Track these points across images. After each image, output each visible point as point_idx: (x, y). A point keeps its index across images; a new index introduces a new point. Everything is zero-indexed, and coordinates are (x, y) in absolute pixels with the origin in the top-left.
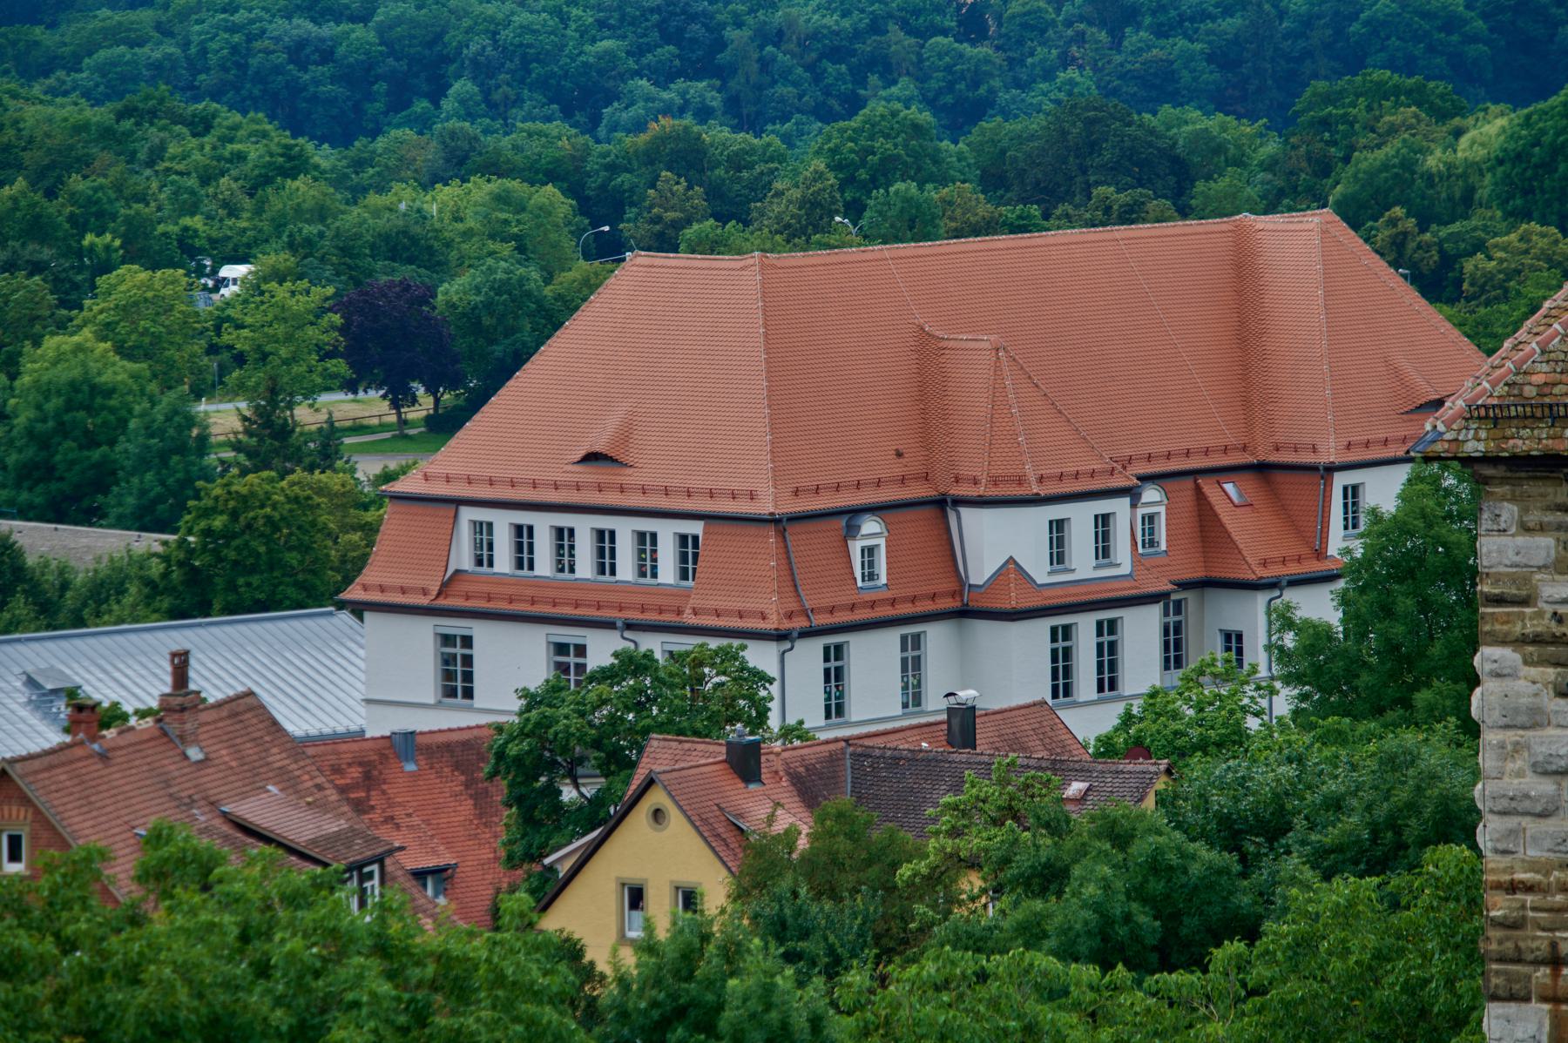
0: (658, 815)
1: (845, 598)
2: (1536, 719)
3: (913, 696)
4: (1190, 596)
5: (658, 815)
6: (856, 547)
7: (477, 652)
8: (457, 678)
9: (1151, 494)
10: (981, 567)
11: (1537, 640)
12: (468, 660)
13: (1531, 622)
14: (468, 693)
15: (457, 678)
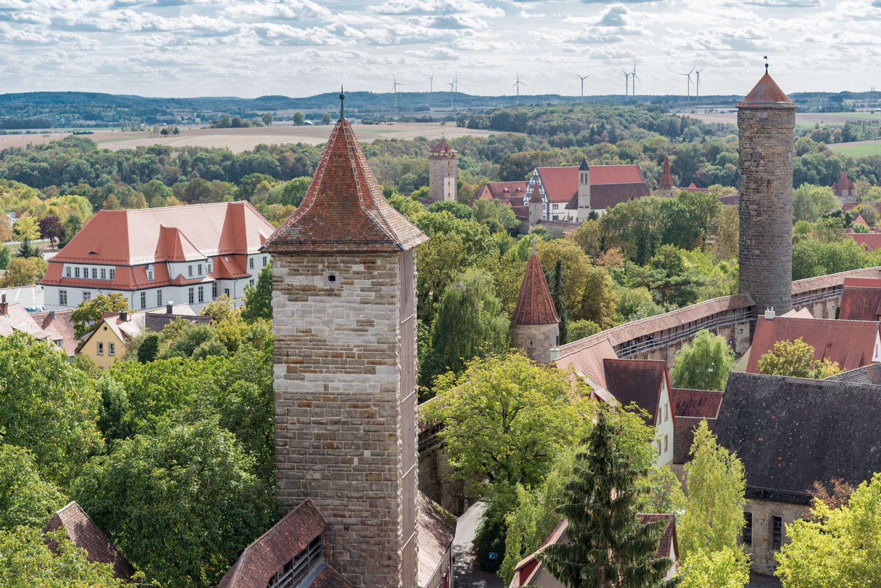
2: (284, 306)
5: (106, 329)
6: (147, 271)
8: (63, 301)
9: (210, 260)
10: (174, 277)
13: (283, 285)
15: (63, 301)
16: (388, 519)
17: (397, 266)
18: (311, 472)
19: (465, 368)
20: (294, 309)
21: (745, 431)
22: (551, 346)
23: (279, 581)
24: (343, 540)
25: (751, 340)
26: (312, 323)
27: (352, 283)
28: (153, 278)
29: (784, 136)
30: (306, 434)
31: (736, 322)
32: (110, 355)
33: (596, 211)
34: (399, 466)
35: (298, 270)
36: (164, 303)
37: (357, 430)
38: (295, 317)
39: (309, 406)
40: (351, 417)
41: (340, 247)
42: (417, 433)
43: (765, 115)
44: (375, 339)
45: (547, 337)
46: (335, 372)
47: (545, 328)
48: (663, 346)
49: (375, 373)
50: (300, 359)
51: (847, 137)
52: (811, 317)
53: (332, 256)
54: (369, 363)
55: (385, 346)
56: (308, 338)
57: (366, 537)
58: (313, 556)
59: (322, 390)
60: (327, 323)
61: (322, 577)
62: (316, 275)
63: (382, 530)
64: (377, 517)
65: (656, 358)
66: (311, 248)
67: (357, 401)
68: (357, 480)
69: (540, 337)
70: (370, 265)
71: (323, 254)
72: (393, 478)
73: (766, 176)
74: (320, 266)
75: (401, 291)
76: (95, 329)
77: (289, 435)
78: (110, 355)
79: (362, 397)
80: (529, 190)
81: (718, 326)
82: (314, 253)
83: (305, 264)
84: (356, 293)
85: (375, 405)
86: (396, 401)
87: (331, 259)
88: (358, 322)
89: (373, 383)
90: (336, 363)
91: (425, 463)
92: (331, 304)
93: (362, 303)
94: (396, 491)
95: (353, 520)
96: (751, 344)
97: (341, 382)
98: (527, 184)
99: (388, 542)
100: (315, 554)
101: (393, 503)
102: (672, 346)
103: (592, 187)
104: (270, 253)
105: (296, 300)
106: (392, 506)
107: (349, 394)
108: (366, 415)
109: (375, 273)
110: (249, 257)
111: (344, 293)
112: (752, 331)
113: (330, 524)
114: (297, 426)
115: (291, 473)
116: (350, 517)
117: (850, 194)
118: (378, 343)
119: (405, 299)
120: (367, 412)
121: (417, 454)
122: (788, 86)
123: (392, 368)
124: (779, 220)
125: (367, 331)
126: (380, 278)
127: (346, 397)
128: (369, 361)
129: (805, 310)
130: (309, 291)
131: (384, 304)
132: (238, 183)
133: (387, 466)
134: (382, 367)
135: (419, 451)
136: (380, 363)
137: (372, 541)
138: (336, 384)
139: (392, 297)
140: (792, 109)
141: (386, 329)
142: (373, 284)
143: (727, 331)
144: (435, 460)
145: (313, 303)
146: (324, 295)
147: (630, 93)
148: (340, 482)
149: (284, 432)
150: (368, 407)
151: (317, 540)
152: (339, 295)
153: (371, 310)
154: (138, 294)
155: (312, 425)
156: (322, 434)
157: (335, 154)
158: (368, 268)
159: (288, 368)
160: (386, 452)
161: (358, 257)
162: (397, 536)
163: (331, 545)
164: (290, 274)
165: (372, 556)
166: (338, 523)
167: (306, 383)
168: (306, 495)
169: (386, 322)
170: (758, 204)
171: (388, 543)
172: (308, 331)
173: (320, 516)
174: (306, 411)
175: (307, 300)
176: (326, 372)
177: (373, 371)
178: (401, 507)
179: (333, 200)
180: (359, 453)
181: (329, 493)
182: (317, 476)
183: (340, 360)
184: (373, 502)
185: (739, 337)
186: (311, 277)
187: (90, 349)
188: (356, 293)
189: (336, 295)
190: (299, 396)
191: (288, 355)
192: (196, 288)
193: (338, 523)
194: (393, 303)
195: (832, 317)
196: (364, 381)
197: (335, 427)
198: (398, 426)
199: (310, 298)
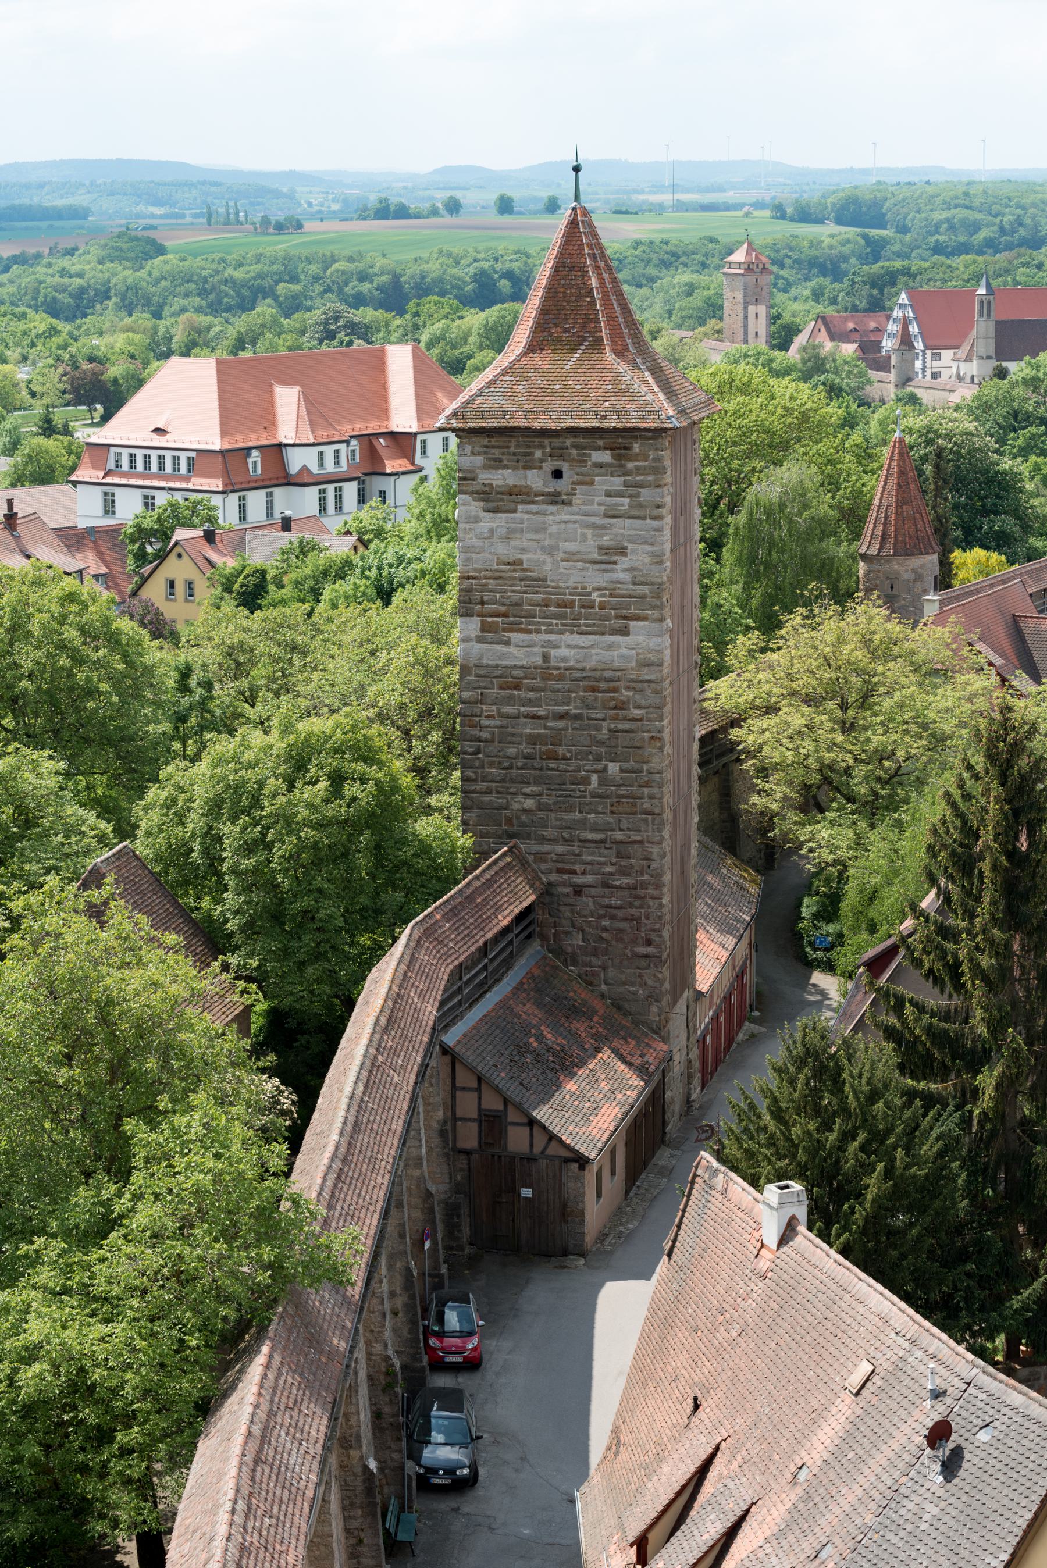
0: (180, 556)
2: (477, 520)
3: (270, 513)
4: (367, 478)
5: (180, 556)
6: (250, 461)
7: (116, 498)
8: (109, 506)
9: (354, 442)
10: (294, 468)
11: (477, 493)
12: (113, 501)
13: (476, 486)
14: (114, 513)
15: (109, 506)
16: (646, 877)
17: (666, 454)
18: (520, 798)
19: (780, 625)
20: (494, 525)
22: (926, 592)
23: (465, 978)
24: (572, 911)
26: (523, 550)
27: (591, 483)
28: (259, 472)
30: (513, 735)
32: (186, 601)
33: (1004, 364)
34: (665, 790)
35: (501, 460)
36: (278, 516)
37: (598, 729)
38: (494, 540)
39: (517, 687)
40: (588, 707)
41: (569, 423)
42: (698, 735)
44: (626, 577)
45: (919, 577)
46: (562, 632)
47: (916, 562)
49: (627, 634)
50: (503, 609)
53: (558, 436)
54: (617, 617)
55: (646, 590)
56: (516, 575)
58: (522, 936)
60: (550, 551)
61: (537, 972)
62: (531, 468)
63: (637, 897)
64: (628, 875)
66: (523, 424)
67: (598, 680)
68: (597, 812)
69: (906, 576)
71: (544, 432)
72: (657, 811)
74: (538, 454)
75: (673, 496)
76: (162, 556)
77: (484, 735)
78: (186, 601)
79: (608, 674)
80: (892, 327)
82: (529, 431)
83: (512, 449)
84: (597, 499)
85: (628, 688)
86: (662, 681)
87: (557, 442)
88: (600, 548)
89: (624, 651)
90: (563, 616)
92: (555, 517)
93: (607, 516)
94: (660, 830)
95: (589, 879)
97: (570, 648)
98: (888, 317)
99: (647, 918)
100: (526, 933)
101: (655, 850)
103: (1000, 326)
104: (453, 430)
106: (655, 856)
107: (583, 669)
109: (630, 465)
110: (419, 438)
111: (576, 500)
113: (550, 884)
114: (497, 722)
115: (486, 799)
116: (584, 873)
118: (634, 584)
119: (681, 511)
120: (613, 699)
121: (696, 771)
123: (656, 625)
125: (615, 563)
126: (638, 474)
127: (579, 675)
128: (617, 614)
130: (516, 495)
131: (644, 518)
132: (401, 312)
133: (646, 790)
135: (700, 765)
136: (637, 618)
137: (620, 914)
138: (564, 652)
139: (658, 507)
141: (647, 560)
142: (626, 485)
144: (727, 780)
145: (526, 516)
146: (544, 502)
148: (567, 816)
149: (475, 732)
150: (615, 690)
151: (528, 910)
152: (569, 503)
153: (623, 528)
154: (233, 499)
156: (539, 735)
158: (618, 457)
160: (645, 767)
161: (601, 438)
162: (661, 906)
163: (552, 920)
164: (486, 467)
165: (621, 940)
166: (564, 884)
167: (512, 649)
168: (511, 836)
169: (648, 548)
171: (647, 918)
172: (516, 564)
173: (533, 870)
174: (511, 697)
175: (515, 511)
176: (547, 632)
177: (625, 632)
178: (668, 858)
180: (600, 767)
181: (549, 833)
182: (529, 803)
183: (571, 612)
184: (622, 849)
186: (522, 472)
187: (154, 592)
188: (597, 499)
189: (563, 503)
191: (482, 603)
192: (331, 489)
193: (564, 884)
194: (659, 518)
196: (610, 647)
197: (561, 724)
198: (665, 722)
199: (520, 507)
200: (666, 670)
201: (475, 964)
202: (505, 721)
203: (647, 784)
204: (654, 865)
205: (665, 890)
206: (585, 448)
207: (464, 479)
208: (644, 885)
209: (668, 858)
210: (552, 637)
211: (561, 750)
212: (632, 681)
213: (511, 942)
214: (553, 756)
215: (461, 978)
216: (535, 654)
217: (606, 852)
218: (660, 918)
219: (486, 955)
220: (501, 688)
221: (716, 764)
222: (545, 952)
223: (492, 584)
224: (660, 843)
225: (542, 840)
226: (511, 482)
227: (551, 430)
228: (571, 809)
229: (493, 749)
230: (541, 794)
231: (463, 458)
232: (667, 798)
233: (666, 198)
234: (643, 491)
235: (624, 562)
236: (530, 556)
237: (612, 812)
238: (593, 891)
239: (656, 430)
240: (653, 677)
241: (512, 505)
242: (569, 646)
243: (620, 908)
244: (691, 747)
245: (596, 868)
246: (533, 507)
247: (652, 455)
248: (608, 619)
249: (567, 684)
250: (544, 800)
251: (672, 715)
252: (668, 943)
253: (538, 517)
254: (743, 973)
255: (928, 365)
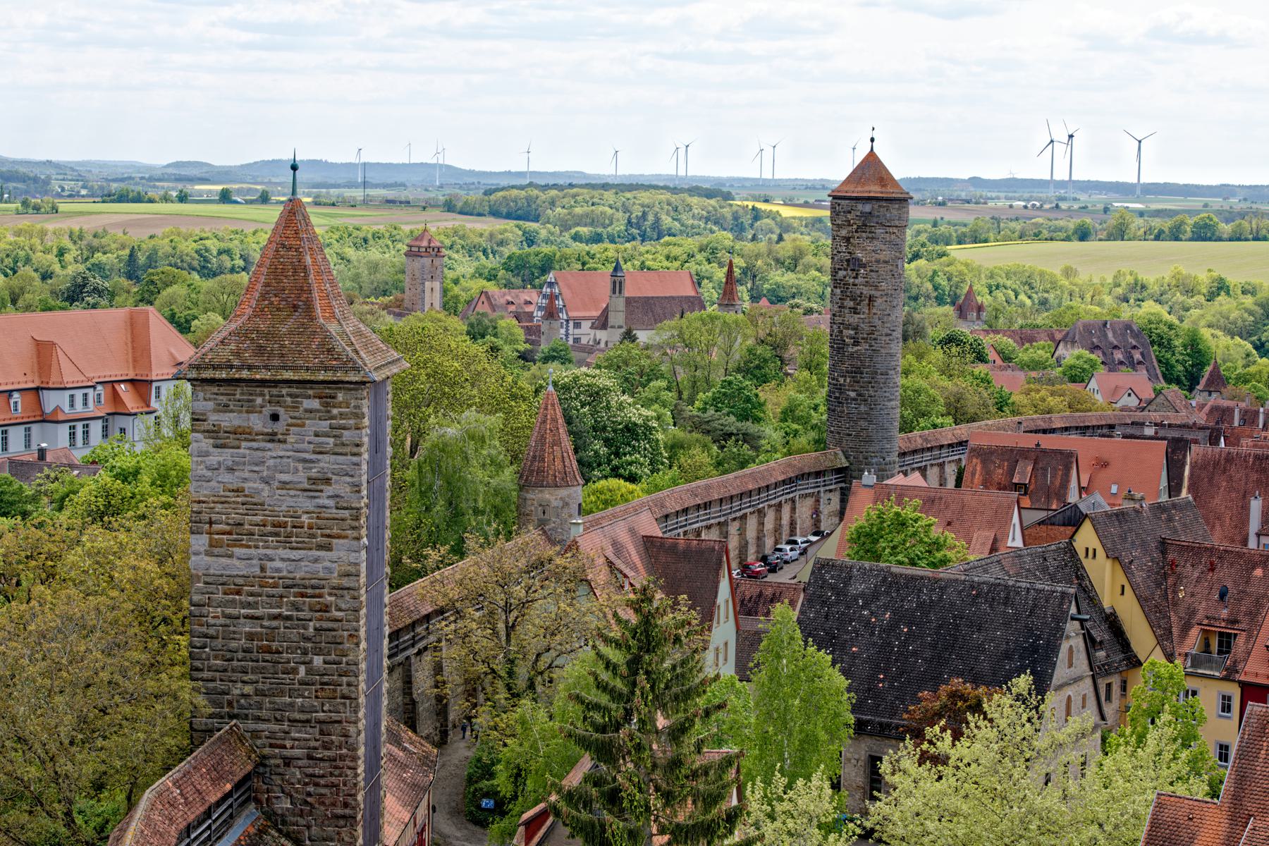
1: (8, 416)
2: (207, 454)
3: (28, 445)
6: (12, 401)
9: (99, 387)
10: (49, 408)
11: (208, 431)
13: (205, 426)
16: (344, 751)
17: (365, 402)
18: (239, 685)
20: (221, 459)
21: (834, 638)
22: (570, 516)
23: (193, 836)
25: (841, 514)
27: (303, 425)
29: (893, 237)
30: (234, 633)
31: (822, 489)
34: (361, 678)
36: (34, 447)
38: (222, 470)
39: (238, 593)
40: (298, 610)
43: (867, 208)
46: (277, 548)
48: (722, 519)
49: (330, 549)
50: (228, 528)
51: (976, 238)
52: (924, 484)
54: (323, 536)
56: (239, 500)
57: (314, 776)
59: (257, 571)
62: (252, 412)
63: (336, 767)
65: (714, 535)
66: (245, 374)
67: (306, 587)
68: (304, 697)
70: (328, 401)
71: (263, 383)
73: (866, 291)
74: (259, 400)
75: (370, 436)
77: (212, 631)
81: (797, 493)
83: (238, 397)
85: (330, 594)
86: (358, 589)
87: (275, 391)
88: (309, 479)
89: (328, 564)
90: (277, 535)
91: (396, 675)
93: (315, 452)
94: (356, 712)
95: (297, 752)
96: (841, 520)
100: (243, 798)
101: (352, 729)
102: (734, 519)
105: (223, 446)
108: (318, 607)
109: (335, 411)
110: (154, 385)
111: (291, 439)
112: (844, 501)
113: (264, 757)
114: (222, 621)
115: (211, 685)
116: (292, 748)
117: (979, 317)
122: (900, 168)
123: (355, 543)
124: (883, 351)
125: (321, 491)
127: (290, 582)
129: (917, 474)
131: (346, 454)
133: (345, 679)
134: (341, 541)
135: (390, 657)
136: (339, 537)
137: (322, 782)
138: (278, 564)
139: (358, 445)
140: (905, 200)
141: (348, 490)
143: (810, 502)
147: (682, 173)
148: (277, 700)
149: (204, 629)
151: (247, 778)
152: (285, 442)
155: (242, 620)
156: (256, 633)
157: (284, 246)
158: (327, 405)
159: (211, 539)
160: (344, 659)
164: (215, 411)
165: (323, 803)
167: (235, 562)
168: (232, 717)
169: (348, 479)
170: (855, 329)
171: (345, 785)
174: (234, 601)
175: (239, 448)
176: (265, 547)
177: (328, 548)
178: (363, 735)
179: (279, 309)
180: (307, 659)
181: (264, 714)
182: (248, 689)
183: (282, 531)
184: (324, 726)
185: (825, 509)
189: (280, 441)
190: (225, 579)
191: (211, 523)
195: (951, 484)
196: (316, 560)
197: (275, 623)
199: (244, 444)
200: (363, 580)
201: (200, 824)
202: (228, 621)
203: (345, 674)
204: (351, 740)
205: (360, 762)
206: (297, 396)
207: (198, 420)
208: (342, 758)
209: (363, 735)
210: (269, 552)
211: (275, 645)
212: (334, 588)
213: (231, 806)
214: (269, 650)
215: (189, 836)
216: (253, 566)
217: (311, 730)
218: (355, 785)
219: (210, 817)
220: (225, 593)
221: (400, 658)
222: (258, 814)
223: (219, 507)
224: (355, 723)
225: (258, 719)
226: (236, 423)
227: (270, 381)
228: (282, 694)
229: (219, 643)
230: (257, 682)
231: (196, 404)
232: (363, 686)
233: (358, 194)
234: (346, 433)
235: (329, 490)
236: (251, 485)
237: (317, 697)
238: (300, 763)
239: (356, 383)
240: (352, 585)
241: (237, 442)
242: (282, 560)
243: (323, 776)
244: (382, 644)
245: (302, 743)
246: (255, 445)
247: (353, 403)
248: (313, 536)
249: (280, 590)
250: (260, 686)
251: (367, 616)
252: (362, 806)
253: (259, 454)
254: (423, 830)
255: (571, 332)
